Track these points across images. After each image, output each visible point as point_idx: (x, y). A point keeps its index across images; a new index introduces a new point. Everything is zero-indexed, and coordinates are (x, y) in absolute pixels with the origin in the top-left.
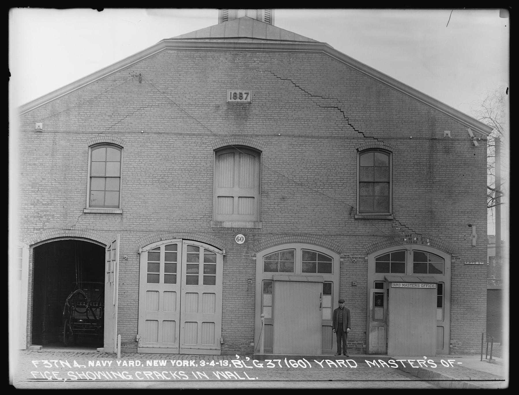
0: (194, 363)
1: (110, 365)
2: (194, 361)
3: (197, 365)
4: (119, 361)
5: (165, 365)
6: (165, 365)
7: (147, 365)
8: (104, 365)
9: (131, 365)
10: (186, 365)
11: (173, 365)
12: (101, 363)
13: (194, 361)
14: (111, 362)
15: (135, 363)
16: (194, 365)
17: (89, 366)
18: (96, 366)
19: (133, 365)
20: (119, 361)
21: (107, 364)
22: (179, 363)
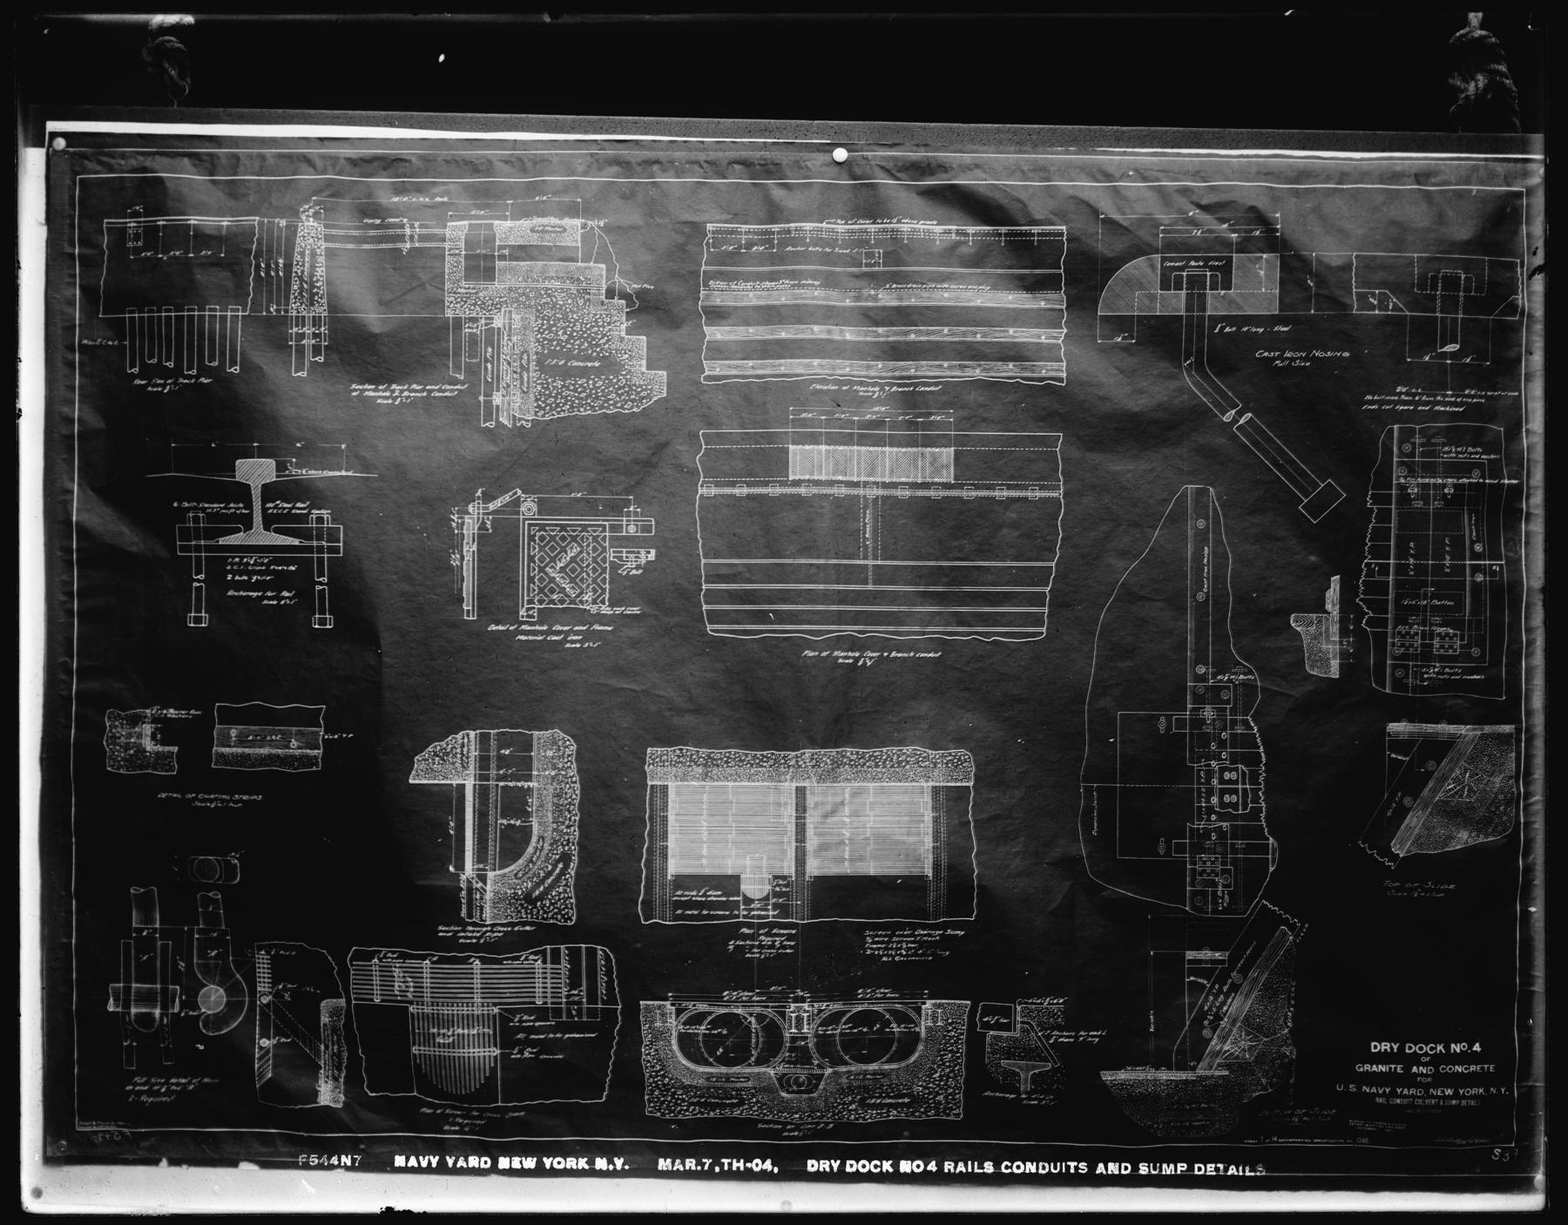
1: (434, 1165)
2: (586, 1159)
13: (586, 1159)
21: (429, 1160)
22: (559, 1163)
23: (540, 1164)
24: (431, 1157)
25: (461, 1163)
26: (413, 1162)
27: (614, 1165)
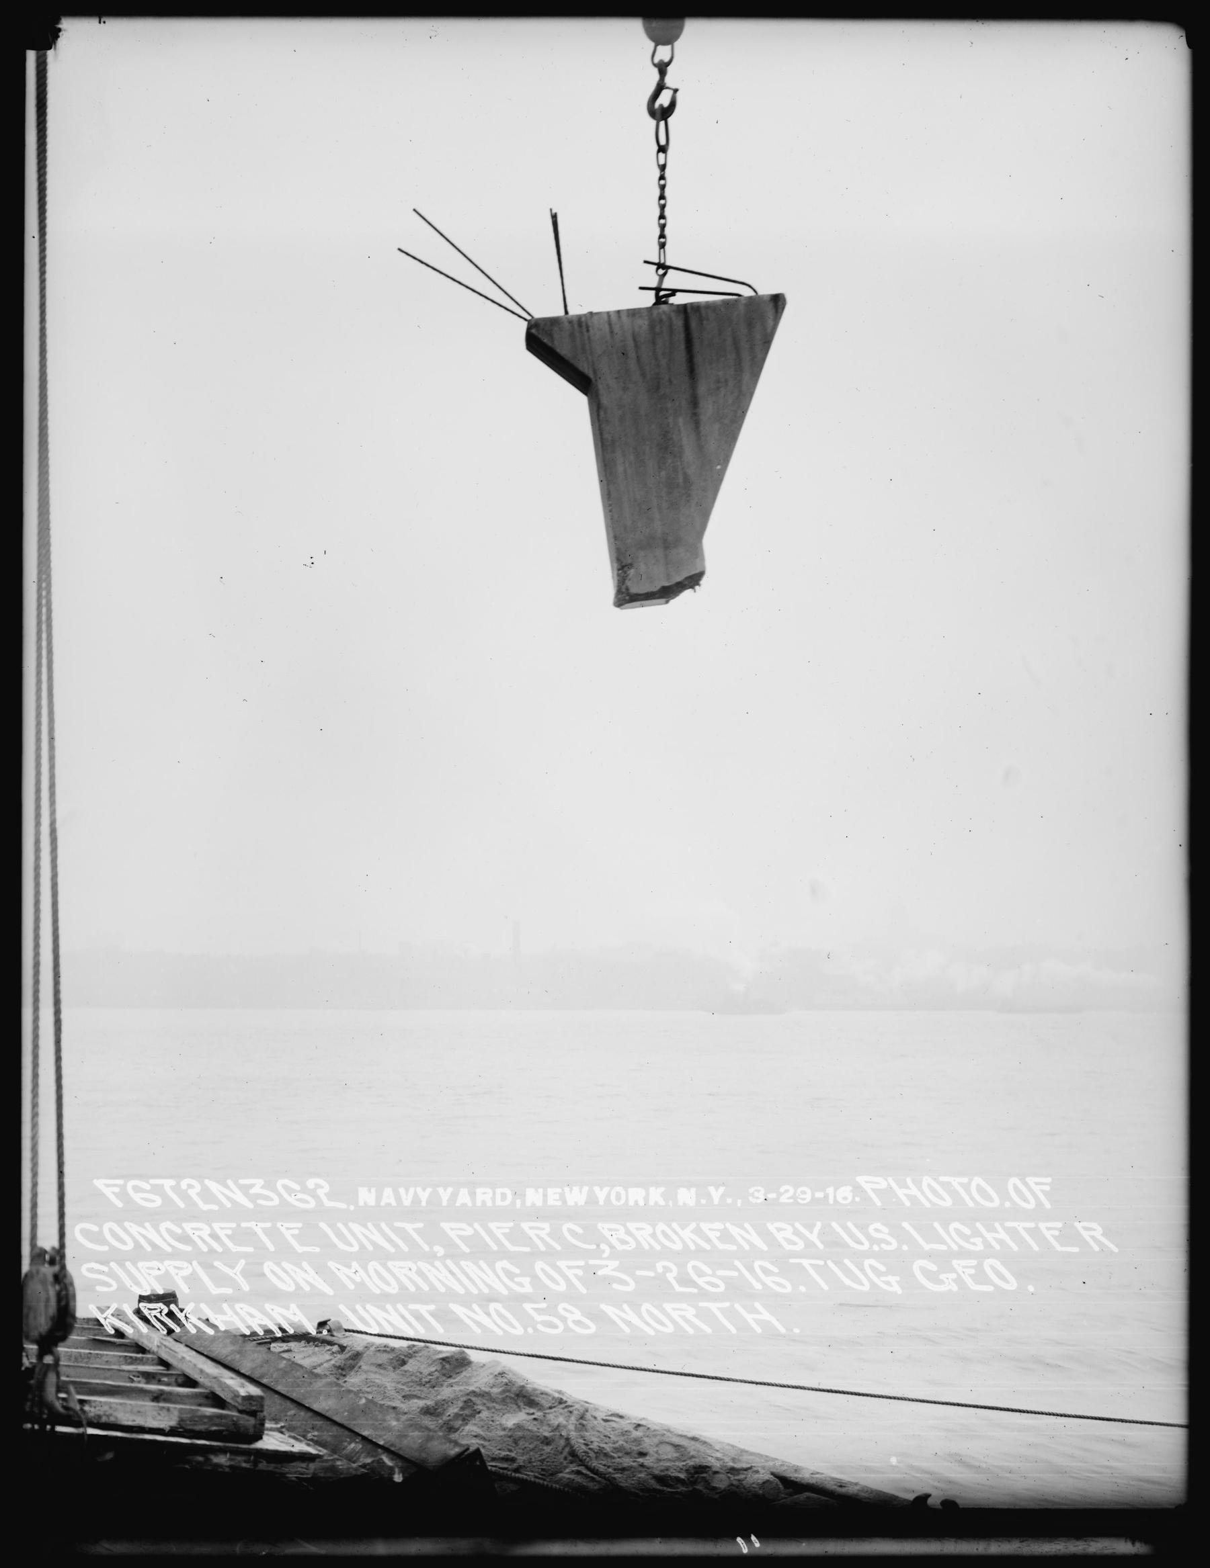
0: (663, 1195)
1: (424, 1204)
2: (662, 1189)
3: (671, 1203)
4: (445, 1190)
6: (581, 1202)
7: (528, 1204)
8: (407, 1202)
9: (484, 1202)
11: (601, 1203)
12: (398, 1198)
13: (662, 1189)
14: (429, 1190)
15: (494, 1193)
16: (662, 1203)
17: (361, 1203)
18: (383, 1204)
19: (489, 1204)
20: (445, 1190)
21: (415, 1193)
22: (618, 1197)
24: (419, 1190)
25: (464, 1198)
26: (388, 1196)
27: (709, 1196)
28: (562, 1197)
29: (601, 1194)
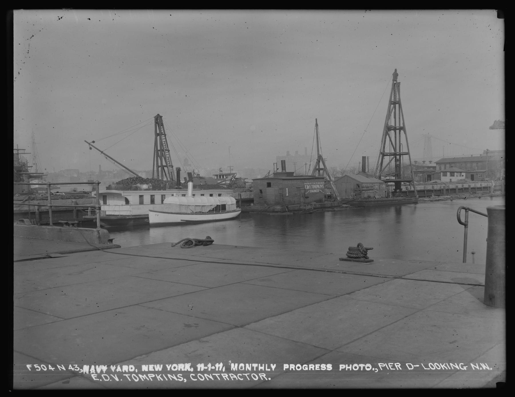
5: (160, 369)
6: (160, 369)
10: (181, 369)
11: (169, 370)
22: (175, 368)
23: (165, 368)
28: (154, 368)
29: (168, 367)
